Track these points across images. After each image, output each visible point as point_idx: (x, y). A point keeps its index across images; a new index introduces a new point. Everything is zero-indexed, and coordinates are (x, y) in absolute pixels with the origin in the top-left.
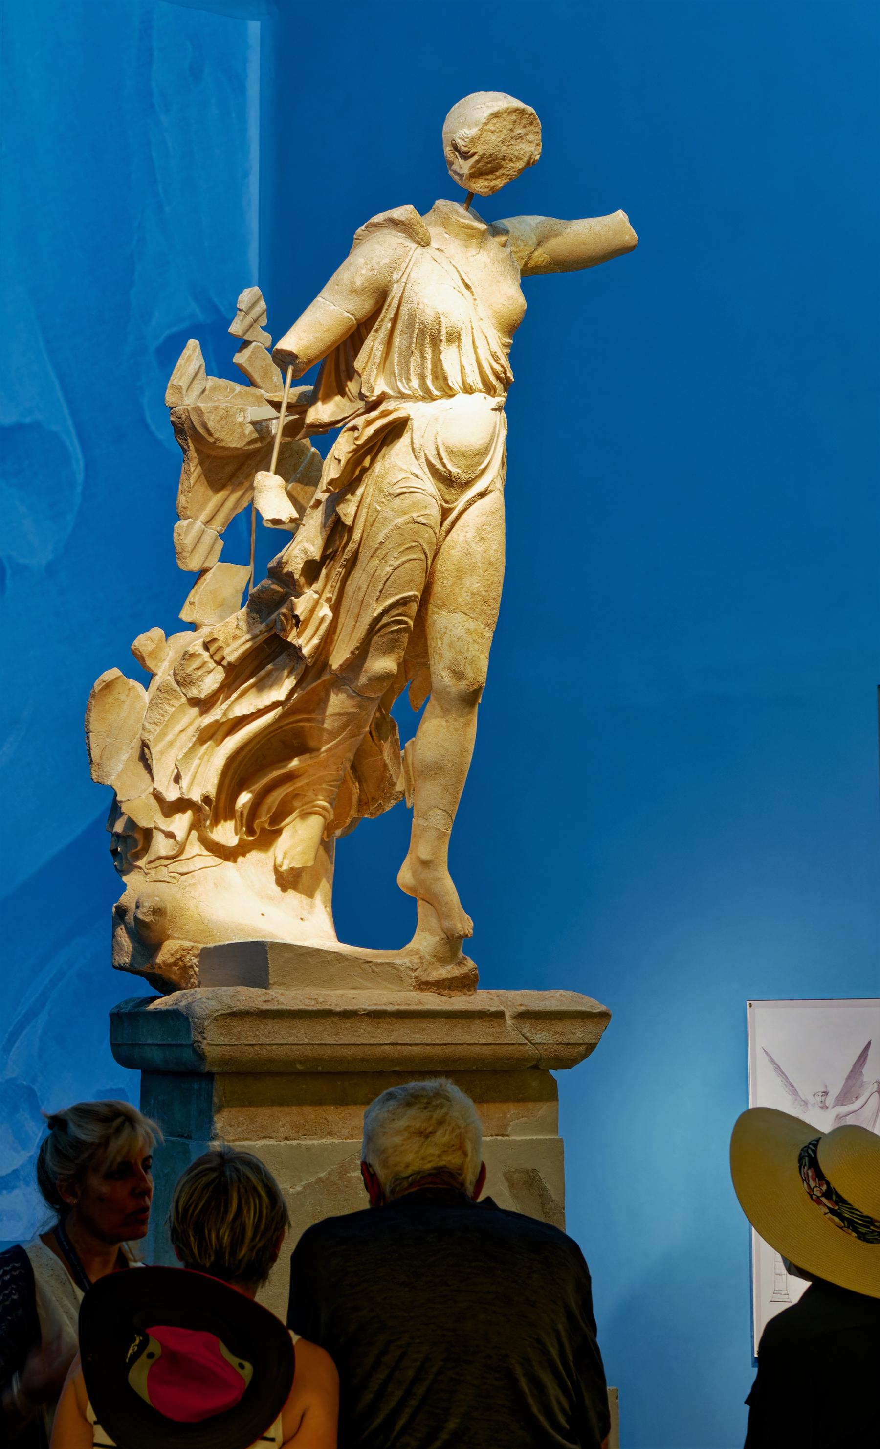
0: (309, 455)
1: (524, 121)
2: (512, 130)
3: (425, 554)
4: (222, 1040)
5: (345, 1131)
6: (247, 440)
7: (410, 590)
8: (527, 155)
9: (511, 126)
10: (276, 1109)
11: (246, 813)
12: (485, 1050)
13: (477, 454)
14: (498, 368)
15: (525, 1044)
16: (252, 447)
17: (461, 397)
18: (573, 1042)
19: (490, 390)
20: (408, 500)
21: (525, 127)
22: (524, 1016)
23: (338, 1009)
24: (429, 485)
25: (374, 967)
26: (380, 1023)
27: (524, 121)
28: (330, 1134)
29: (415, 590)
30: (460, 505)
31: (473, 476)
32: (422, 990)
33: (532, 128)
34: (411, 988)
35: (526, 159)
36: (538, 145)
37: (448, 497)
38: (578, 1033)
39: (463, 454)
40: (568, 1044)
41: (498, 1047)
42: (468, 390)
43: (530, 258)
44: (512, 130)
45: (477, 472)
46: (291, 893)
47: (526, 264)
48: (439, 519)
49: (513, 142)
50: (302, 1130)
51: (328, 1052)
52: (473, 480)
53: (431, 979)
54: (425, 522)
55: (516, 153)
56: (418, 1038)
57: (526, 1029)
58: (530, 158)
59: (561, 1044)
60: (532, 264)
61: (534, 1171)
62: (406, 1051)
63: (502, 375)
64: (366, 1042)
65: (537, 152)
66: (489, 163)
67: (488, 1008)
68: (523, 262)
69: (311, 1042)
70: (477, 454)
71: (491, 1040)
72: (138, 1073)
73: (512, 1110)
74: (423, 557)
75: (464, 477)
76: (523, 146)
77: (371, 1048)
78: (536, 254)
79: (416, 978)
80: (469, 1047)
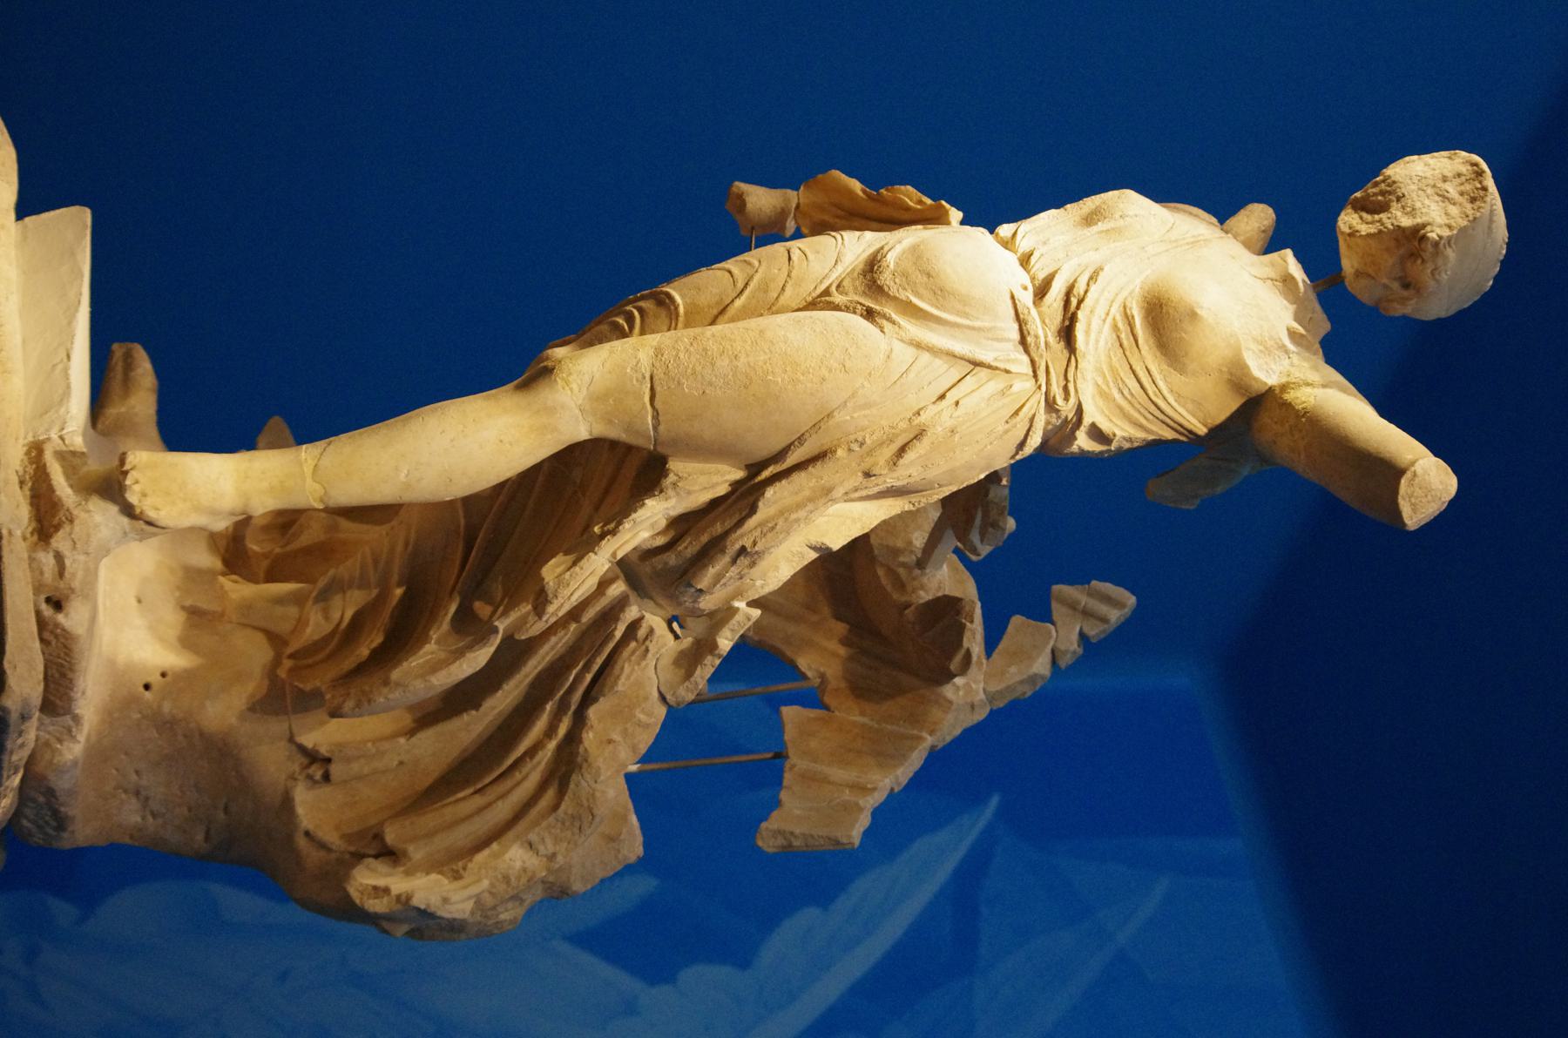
1: (1468, 187)
2: (1445, 179)
7: (683, 297)
8: (1424, 219)
9: (1449, 175)
13: (929, 275)
14: (1080, 288)
17: (1011, 259)
19: (1041, 292)
21: (1462, 194)
25: (60, 367)
27: (1468, 187)
31: (893, 291)
32: (28, 453)
33: (1469, 206)
34: (30, 438)
35: (1419, 220)
36: (1450, 227)
39: (919, 257)
42: (1025, 261)
43: (1297, 385)
44: (1445, 179)
45: (903, 295)
46: (181, 617)
47: (1284, 387)
48: (809, 290)
49: (1430, 191)
52: (888, 295)
54: (794, 258)
55: (1418, 205)
58: (1424, 226)
60: (1290, 396)
63: (1074, 302)
65: (1438, 231)
66: (1383, 193)
68: (1284, 380)
70: (929, 275)
74: (740, 285)
75: (885, 279)
76: (1433, 206)
78: (1309, 390)
79: (49, 439)
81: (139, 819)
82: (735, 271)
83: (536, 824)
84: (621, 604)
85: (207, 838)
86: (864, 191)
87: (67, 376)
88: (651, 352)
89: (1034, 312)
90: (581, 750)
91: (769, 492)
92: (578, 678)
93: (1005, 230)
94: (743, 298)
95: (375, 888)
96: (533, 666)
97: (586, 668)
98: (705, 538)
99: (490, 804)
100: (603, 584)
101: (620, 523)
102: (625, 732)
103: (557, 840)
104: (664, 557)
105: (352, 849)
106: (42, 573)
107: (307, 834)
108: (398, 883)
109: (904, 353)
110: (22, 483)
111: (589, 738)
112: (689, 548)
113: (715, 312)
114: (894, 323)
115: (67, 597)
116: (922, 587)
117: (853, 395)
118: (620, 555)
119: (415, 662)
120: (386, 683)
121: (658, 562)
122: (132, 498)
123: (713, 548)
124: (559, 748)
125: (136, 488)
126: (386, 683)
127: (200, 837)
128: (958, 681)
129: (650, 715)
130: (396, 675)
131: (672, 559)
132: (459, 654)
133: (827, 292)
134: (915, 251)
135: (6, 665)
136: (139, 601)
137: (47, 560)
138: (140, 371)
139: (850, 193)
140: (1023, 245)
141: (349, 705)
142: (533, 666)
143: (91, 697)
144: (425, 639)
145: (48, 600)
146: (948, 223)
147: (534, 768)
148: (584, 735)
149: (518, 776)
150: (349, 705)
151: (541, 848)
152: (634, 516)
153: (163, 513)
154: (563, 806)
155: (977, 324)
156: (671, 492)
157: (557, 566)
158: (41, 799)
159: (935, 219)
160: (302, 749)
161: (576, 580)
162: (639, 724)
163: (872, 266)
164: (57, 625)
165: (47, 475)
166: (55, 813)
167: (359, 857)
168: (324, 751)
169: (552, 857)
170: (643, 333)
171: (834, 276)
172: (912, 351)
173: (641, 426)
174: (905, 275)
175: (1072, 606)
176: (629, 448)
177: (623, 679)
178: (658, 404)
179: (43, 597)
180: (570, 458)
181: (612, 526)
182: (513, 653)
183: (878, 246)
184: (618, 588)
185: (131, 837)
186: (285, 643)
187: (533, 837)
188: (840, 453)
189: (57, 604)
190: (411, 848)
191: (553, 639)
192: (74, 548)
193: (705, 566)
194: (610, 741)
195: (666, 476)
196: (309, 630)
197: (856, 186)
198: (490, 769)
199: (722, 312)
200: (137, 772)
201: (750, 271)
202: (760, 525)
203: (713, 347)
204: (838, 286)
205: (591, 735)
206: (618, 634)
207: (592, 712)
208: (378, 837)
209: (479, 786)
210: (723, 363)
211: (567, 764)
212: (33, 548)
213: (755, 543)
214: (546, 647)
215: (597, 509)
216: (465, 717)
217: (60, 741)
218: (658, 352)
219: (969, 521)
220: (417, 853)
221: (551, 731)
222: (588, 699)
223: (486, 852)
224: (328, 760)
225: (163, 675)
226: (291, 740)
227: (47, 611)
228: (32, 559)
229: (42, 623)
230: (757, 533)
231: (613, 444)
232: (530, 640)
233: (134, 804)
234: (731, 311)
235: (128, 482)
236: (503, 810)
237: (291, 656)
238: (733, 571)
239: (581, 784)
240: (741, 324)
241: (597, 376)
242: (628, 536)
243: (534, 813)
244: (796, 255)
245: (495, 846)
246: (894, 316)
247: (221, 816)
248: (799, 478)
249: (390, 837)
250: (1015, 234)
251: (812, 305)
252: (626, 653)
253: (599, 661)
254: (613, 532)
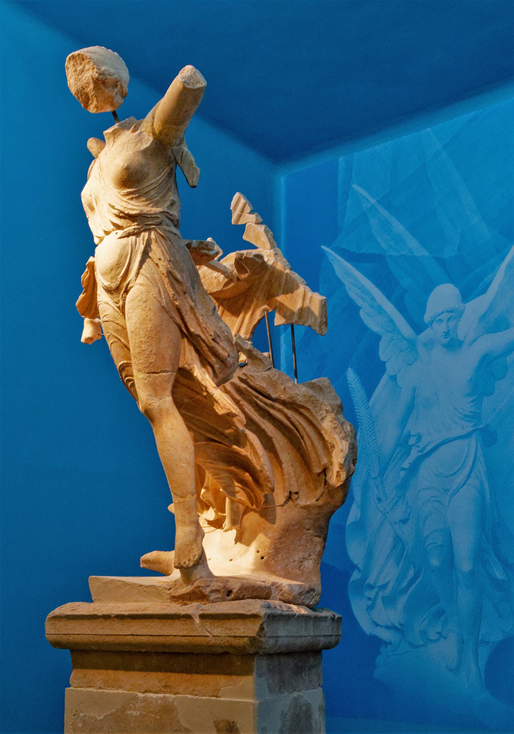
0: (284, 276)
3: (116, 337)
4: (52, 631)
5: (181, 689)
6: (223, 284)
7: (121, 361)
10: (95, 671)
12: (184, 640)
15: (208, 636)
16: (229, 287)
18: (238, 635)
22: (203, 617)
23: (101, 614)
25: (145, 589)
26: (124, 622)
28: (121, 687)
29: (123, 360)
34: (169, 601)
37: (115, 300)
40: (235, 637)
41: (191, 638)
48: (119, 315)
50: (107, 684)
51: (101, 639)
52: (119, 285)
53: (176, 595)
56: (145, 631)
59: (229, 636)
61: (233, 722)
62: (140, 639)
64: (117, 633)
67: (180, 612)
69: (92, 633)
70: (112, 269)
71: (186, 633)
72: (69, 650)
73: (222, 680)
74: (116, 340)
75: (114, 286)
77: (121, 637)
79: (169, 594)
80: (174, 638)
81: (311, 561)
82: (111, 341)
83: (314, 416)
84: (233, 385)
85: (319, 537)
86: (83, 294)
87: (147, 587)
88: (140, 373)
89: (126, 230)
90: (287, 400)
91: (192, 330)
92: (261, 401)
93: (96, 241)
94: (121, 339)
95: (337, 476)
96: (256, 417)
97: (257, 398)
98: (209, 354)
99: (307, 434)
100: (226, 392)
101: (202, 385)
102: (282, 384)
103: (321, 409)
104: (216, 369)
105: (323, 484)
106: (218, 598)
107: (317, 500)
108: (336, 468)
109: (141, 279)
110: (186, 604)
111: (283, 397)
112: (213, 359)
113: (126, 349)
114: (129, 283)
115: (227, 588)
116: (232, 273)
117: (156, 298)
118: (215, 385)
119: (254, 461)
120: (261, 471)
121: (218, 371)
122: (191, 564)
123: (212, 350)
124: (287, 408)
125: (187, 563)
126: (261, 471)
127: (318, 539)
128: (266, 259)
129: (275, 375)
130: (258, 468)
131: (216, 366)
132: (252, 445)
133: (119, 307)
134: (104, 274)
135: (249, 613)
136: (231, 560)
137: (213, 596)
138: (150, 557)
139: (84, 298)
140: (102, 234)
141: (269, 485)
142: (256, 417)
143: (266, 578)
144: (245, 457)
145: (228, 595)
146: (94, 262)
147: (294, 417)
148: (282, 399)
149: (297, 423)
150: (269, 485)
151: (324, 415)
152: (200, 380)
153: (197, 553)
154: (309, 407)
155: (130, 251)
156: (192, 366)
157: (218, 409)
158: (303, 597)
159: (92, 267)
160: (286, 502)
161: (224, 402)
162: (278, 378)
163: (109, 291)
164: (237, 592)
165: (182, 595)
166: (308, 592)
167: (326, 482)
168: (287, 494)
169: (327, 411)
170: (133, 376)
171: (113, 305)
172: (140, 276)
173: (168, 377)
174: (112, 278)
175: (240, 216)
176: (176, 381)
177: (261, 384)
178: (159, 371)
179: (227, 598)
180: (178, 404)
181: (204, 389)
182: (251, 423)
183: (102, 288)
184: (228, 385)
185: (318, 564)
186: (247, 507)
187: (319, 418)
188: (177, 303)
189: (230, 592)
190: (323, 463)
191: (246, 410)
192: (209, 586)
193: (219, 354)
194: (285, 389)
195: (186, 368)
196: (243, 499)
197: (81, 296)
198: (295, 433)
199: (126, 347)
200: (294, 562)
201: (111, 336)
202: (203, 332)
203: (137, 350)
204: (117, 303)
205: (282, 396)
206: (245, 386)
207: (274, 396)
208: (319, 475)
209: (300, 438)
210: (144, 347)
211: (292, 405)
212: (208, 601)
213: (211, 335)
214: (249, 412)
215: (198, 393)
216: (275, 442)
217: (281, 590)
218: (139, 371)
219: (207, 255)
220: (325, 461)
221: (279, 410)
222: (268, 397)
223: (325, 435)
224: (290, 492)
225: (258, 552)
226: (282, 506)
227: (232, 596)
228: (213, 602)
229: (237, 598)
230: (207, 334)
231: (174, 387)
232: (246, 418)
233: (306, 563)
234: (126, 343)
235: (185, 566)
236: (309, 429)
237: (253, 506)
238: (221, 343)
239: (300, 400)
240: (130, 340)
241: (148, 393)
242: (207, 382)
243: (310, 417)
244: (105, 319)
245: (323, 432)
246: (127, 283)
247: (311, 531)
248: (187, 318)
249: (319, 470)
250: (98, 237)
251: (123, 313)
252: (252, 384)
253: (254, 393)
254: (206, 388)
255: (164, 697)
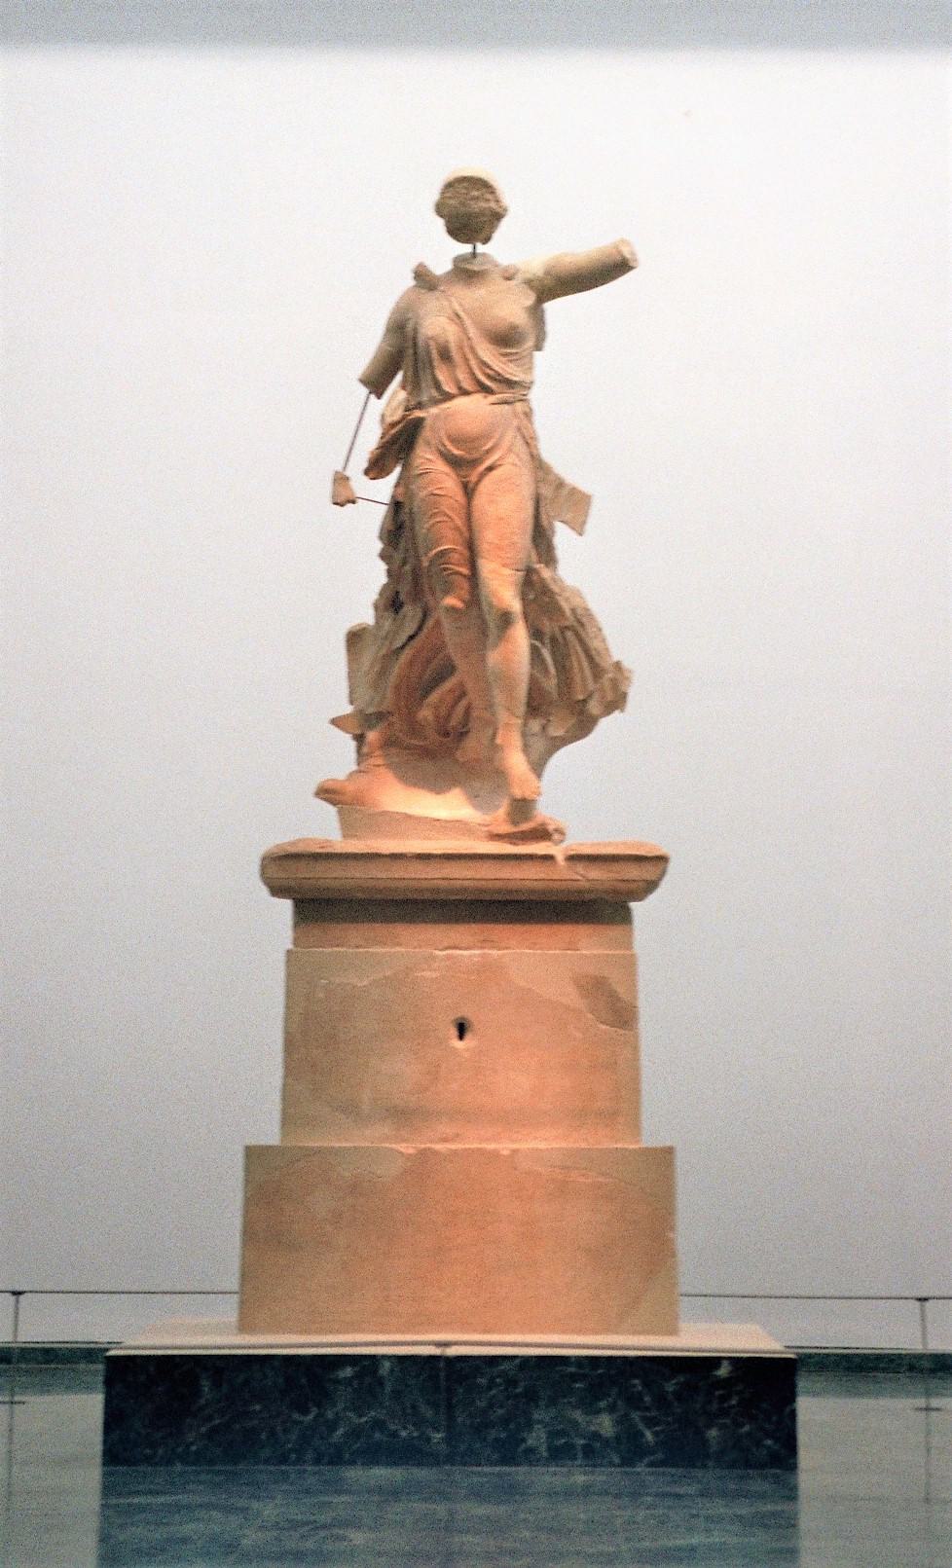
11: (431, 718)
19: (486, 390)
20: (427, 479)
24: (441, 466)
30: (473, 478)
31: (476, 455)
38: (633, 872)
42: (465, 393)
51: (381, 884)
56: (469, 874)
57: (580, 868)
71: (542, 876)
109: (511, 458)
255: (482, 956)
